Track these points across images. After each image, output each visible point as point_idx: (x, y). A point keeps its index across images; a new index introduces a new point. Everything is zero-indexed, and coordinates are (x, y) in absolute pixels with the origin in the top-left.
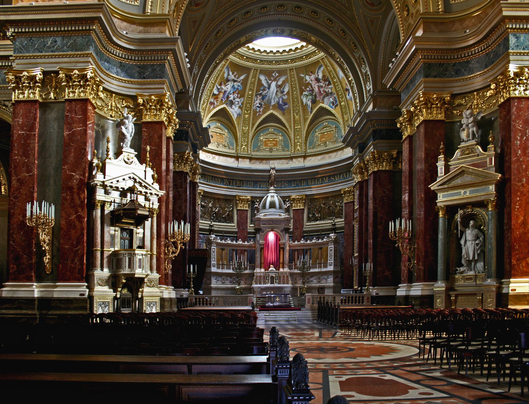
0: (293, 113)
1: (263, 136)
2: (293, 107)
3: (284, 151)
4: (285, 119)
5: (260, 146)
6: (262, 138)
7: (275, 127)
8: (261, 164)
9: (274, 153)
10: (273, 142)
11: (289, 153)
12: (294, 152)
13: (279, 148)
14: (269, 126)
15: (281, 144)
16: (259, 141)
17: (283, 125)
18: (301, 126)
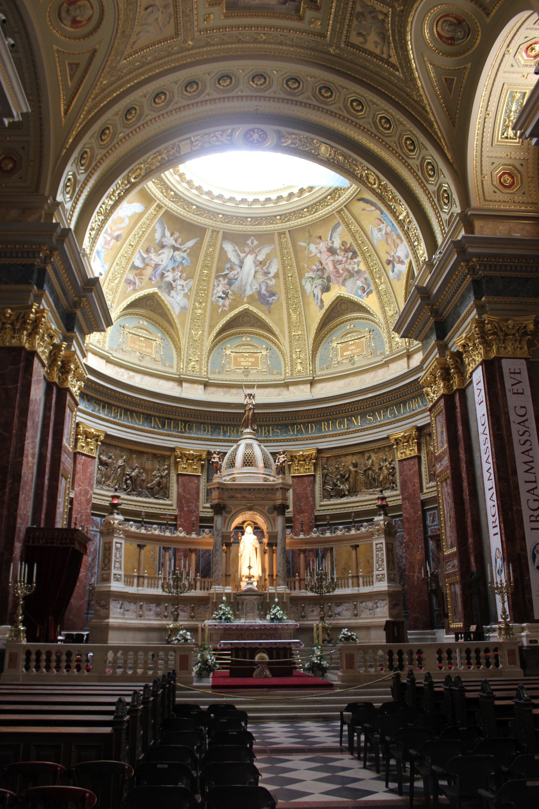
0: (288, 309)
1: (230, 348)
2: (287, 298)
3: (271, 373)
4: (272, 319)
5: (224, 365)
6: (228, 352)
7: (253, 334)
8: (227, 396)
9: (254, 377)
10: (250, 360)
11: (282, 377)
12: (292, 374)
13: (263, 368)
14: (242, 333)
15: (265, 363)
16: (223, 356)
17: (269, 330)
18: (302, 330)
